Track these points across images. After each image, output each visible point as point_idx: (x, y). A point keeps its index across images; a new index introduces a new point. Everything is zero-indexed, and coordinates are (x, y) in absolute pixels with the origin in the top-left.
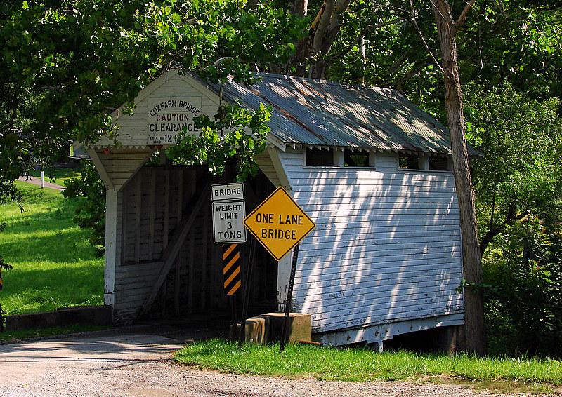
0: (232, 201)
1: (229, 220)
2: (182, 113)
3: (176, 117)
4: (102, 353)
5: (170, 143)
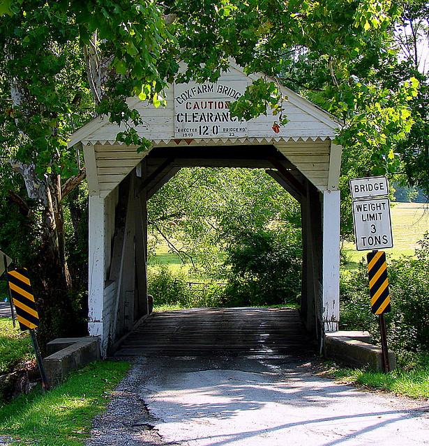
0: (373, 198)
1: (372, 222)
2: (221, 100)
3: (213, 104)
4: (218, 404)
5: (205, 136)
